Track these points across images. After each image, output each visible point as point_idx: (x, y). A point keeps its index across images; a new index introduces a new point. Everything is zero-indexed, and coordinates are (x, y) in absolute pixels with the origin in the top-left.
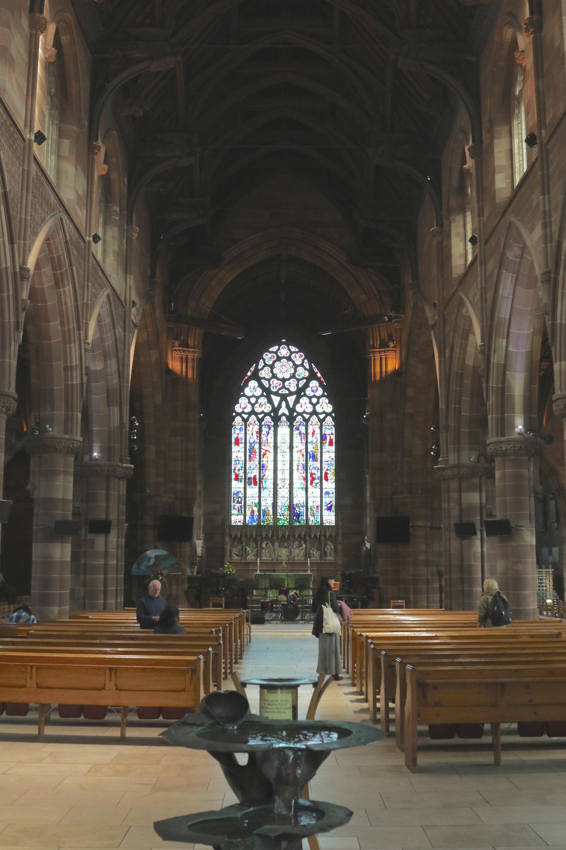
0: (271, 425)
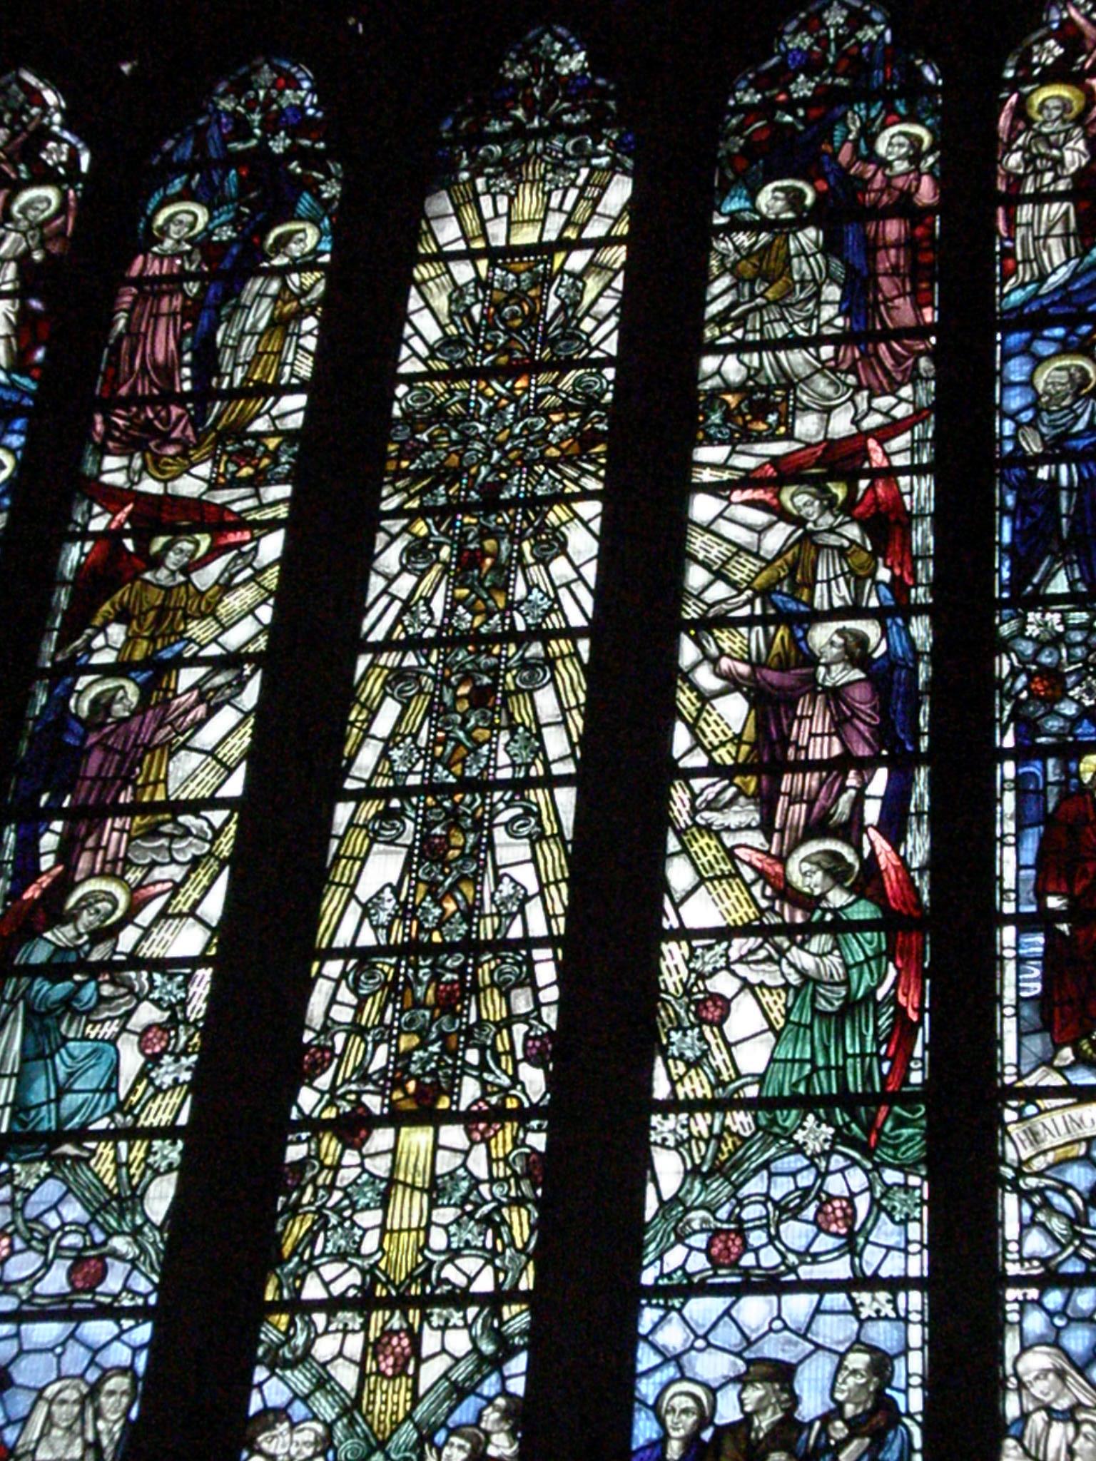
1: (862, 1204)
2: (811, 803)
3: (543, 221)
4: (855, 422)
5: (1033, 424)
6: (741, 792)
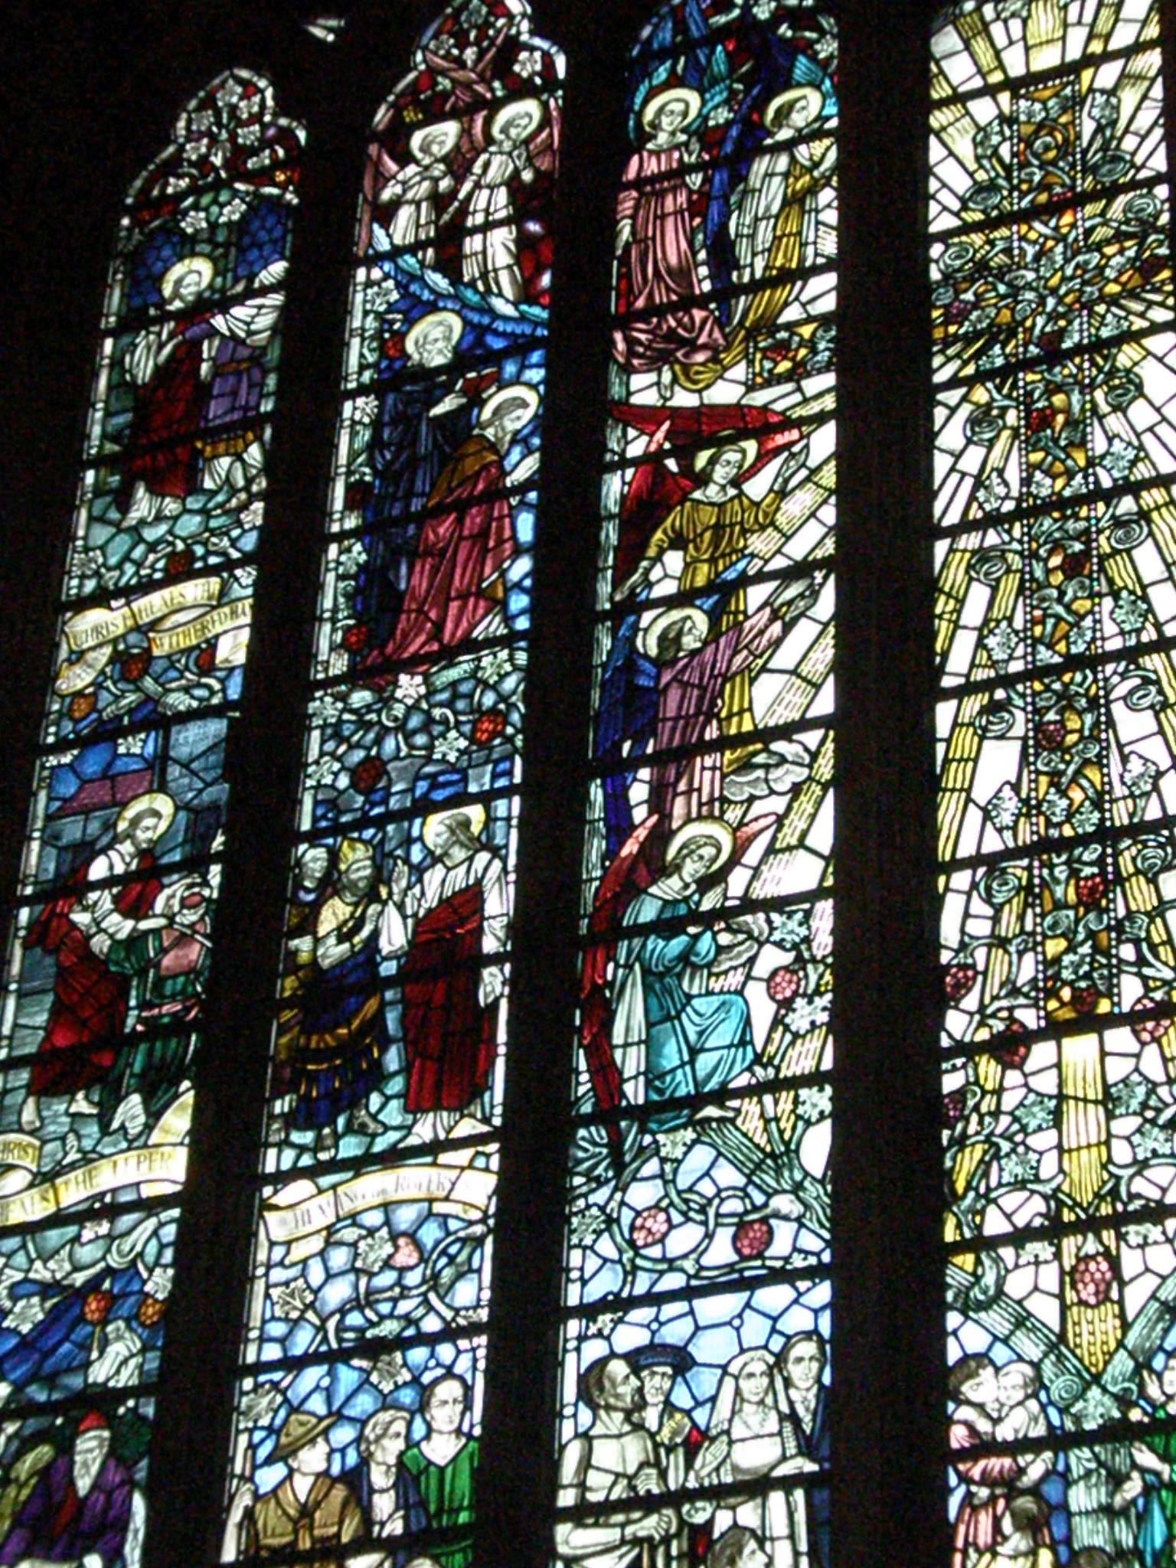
3: (1063, 38)
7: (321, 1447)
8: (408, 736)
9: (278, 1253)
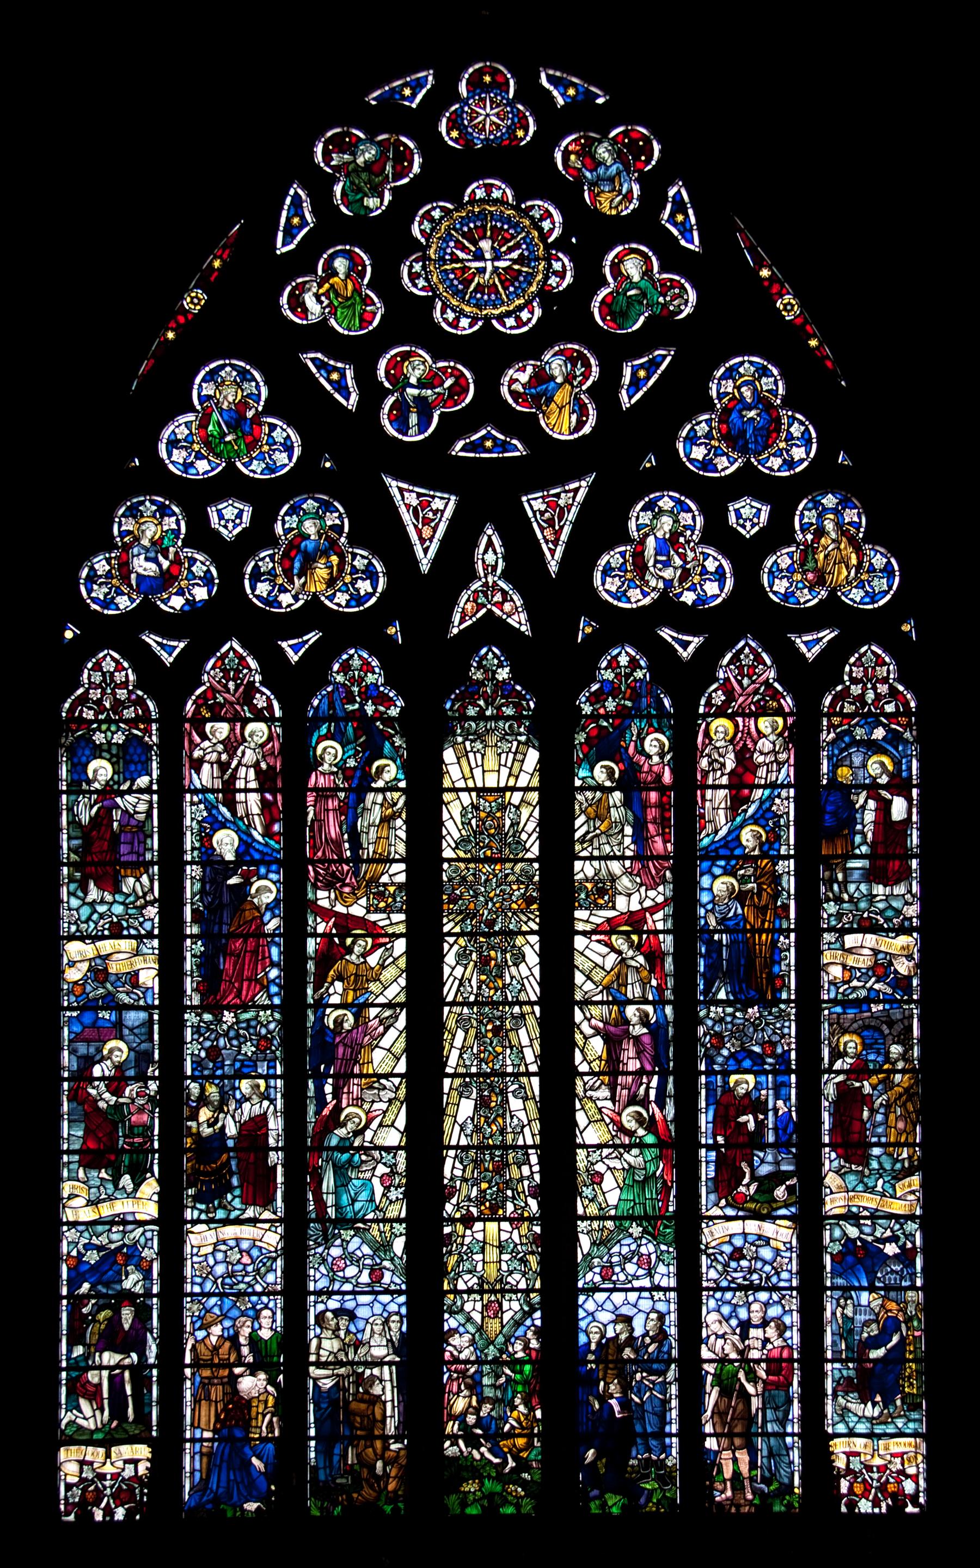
0: (389, 721)
1: (653, 1257)
2: (629, 1090)
3: (499, 771)
4: (641, 903)
5: (712, 911)
6: (602, 1083)
7: (220, 1327)
8: (230, 1040)
9: (195, 1250)
